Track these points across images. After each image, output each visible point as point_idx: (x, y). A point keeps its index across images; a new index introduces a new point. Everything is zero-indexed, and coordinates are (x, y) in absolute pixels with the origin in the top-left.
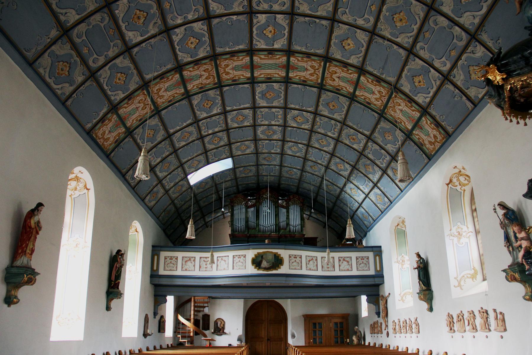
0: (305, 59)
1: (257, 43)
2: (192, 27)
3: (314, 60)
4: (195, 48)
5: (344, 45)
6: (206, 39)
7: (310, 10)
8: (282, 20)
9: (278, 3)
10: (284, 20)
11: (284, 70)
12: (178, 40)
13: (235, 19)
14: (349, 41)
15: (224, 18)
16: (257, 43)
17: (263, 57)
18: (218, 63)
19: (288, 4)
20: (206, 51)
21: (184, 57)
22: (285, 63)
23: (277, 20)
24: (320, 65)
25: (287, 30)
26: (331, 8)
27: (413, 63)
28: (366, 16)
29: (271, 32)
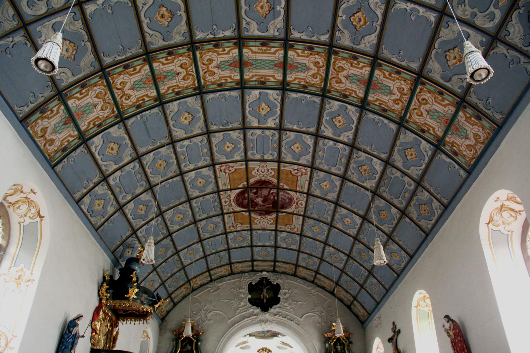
0: (224, 81)
1: (276, 97)
3: (213, 83)
6: (325, 118)
11: (245, 59)
16: (276, 97)
17: (272, 79)
18: (323, 84)
20: (331, 105)
21: (353, 112)
22: (245, 70)
23: (257, 121)
24: (204, 79)
25: (247, 111)
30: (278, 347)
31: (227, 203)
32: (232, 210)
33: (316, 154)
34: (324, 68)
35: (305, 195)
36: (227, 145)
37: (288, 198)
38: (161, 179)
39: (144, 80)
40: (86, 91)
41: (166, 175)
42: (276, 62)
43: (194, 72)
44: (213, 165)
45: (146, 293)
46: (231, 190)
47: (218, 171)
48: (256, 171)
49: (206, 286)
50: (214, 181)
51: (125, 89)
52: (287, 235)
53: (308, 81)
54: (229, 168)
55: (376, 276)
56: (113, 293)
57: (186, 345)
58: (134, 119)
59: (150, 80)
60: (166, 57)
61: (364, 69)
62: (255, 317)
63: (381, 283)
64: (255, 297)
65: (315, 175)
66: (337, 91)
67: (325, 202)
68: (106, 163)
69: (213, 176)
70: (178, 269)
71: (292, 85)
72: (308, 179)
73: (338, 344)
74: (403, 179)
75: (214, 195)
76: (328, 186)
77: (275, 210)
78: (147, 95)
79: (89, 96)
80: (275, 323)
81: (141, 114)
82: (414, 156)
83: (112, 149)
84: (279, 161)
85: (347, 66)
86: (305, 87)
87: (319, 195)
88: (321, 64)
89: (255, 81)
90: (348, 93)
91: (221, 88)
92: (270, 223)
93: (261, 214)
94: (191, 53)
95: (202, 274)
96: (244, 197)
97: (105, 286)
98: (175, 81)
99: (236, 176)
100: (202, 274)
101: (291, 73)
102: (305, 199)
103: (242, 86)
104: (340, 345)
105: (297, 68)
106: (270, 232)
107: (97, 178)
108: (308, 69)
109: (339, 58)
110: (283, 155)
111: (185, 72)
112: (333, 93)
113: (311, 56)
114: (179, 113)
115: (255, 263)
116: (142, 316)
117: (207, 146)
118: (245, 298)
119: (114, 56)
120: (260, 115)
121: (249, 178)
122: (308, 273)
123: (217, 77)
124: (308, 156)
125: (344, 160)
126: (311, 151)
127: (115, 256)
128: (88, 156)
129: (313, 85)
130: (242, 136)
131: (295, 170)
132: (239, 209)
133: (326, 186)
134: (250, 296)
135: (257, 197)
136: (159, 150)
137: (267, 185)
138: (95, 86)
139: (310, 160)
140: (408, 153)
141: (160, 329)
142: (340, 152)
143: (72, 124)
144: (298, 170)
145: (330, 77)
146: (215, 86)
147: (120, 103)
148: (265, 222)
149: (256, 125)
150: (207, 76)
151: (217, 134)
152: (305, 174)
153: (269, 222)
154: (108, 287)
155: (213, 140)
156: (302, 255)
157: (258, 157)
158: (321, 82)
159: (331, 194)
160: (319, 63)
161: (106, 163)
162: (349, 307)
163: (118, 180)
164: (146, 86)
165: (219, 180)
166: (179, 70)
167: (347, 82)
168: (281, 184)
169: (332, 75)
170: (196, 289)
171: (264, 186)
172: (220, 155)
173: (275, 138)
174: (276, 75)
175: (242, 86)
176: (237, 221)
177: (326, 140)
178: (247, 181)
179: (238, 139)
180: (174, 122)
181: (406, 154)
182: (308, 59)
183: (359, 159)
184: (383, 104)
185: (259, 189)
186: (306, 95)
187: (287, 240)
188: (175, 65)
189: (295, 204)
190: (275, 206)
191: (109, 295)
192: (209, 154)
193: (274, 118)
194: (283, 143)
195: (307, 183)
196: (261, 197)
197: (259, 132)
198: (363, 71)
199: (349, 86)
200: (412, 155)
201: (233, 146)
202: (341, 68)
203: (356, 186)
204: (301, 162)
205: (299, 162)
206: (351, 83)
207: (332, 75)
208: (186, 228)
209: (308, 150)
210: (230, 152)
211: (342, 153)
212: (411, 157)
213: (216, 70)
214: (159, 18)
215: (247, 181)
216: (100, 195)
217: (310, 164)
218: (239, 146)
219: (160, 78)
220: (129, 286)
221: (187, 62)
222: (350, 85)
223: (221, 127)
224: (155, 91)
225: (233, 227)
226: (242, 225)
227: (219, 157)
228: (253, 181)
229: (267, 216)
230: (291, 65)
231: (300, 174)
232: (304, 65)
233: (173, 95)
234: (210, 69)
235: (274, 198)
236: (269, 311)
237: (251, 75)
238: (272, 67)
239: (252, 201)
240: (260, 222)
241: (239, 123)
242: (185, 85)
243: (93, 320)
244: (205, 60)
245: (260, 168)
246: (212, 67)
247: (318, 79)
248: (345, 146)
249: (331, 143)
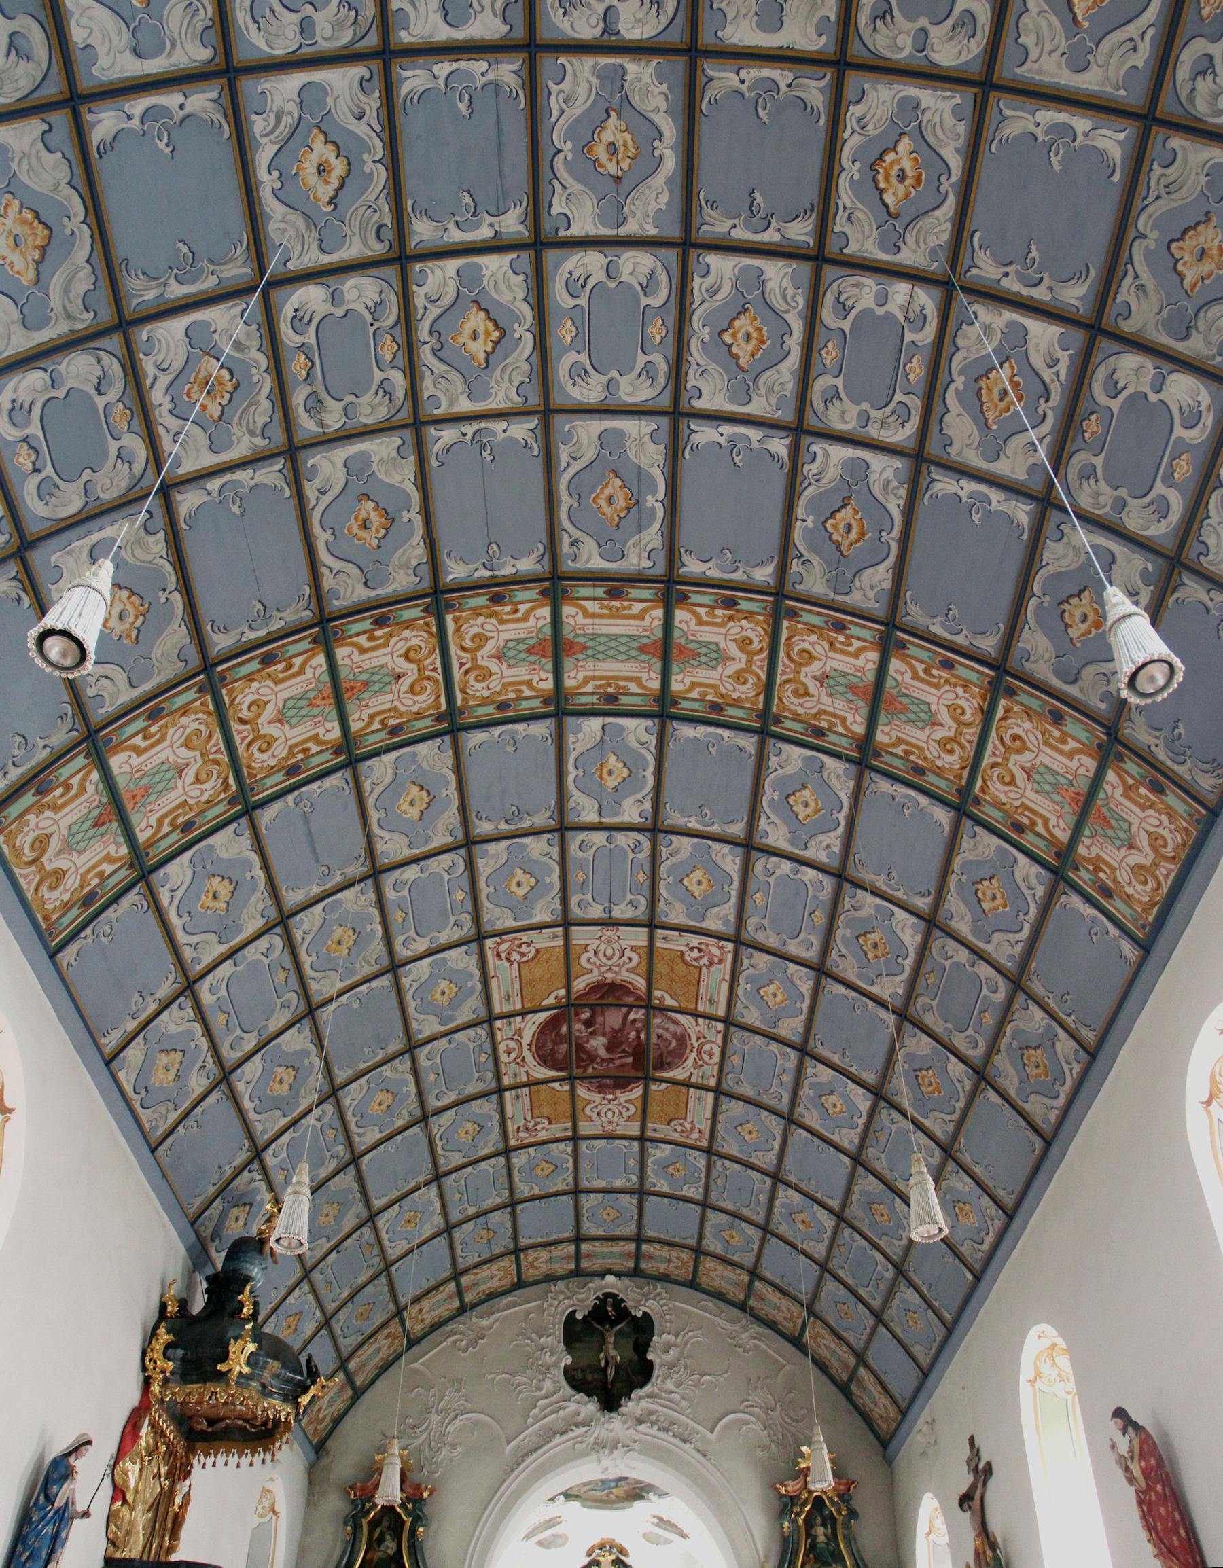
0: (512, 695)
2: (792, 842)
3: (485, 702)
4: (804, 787)
5: (424, 793)
9: (595, 848)
10: (579, 808)
12: (832, 834)
14: (414, 813)
17: (633, 688)
19: (572, 847)
20: (784, 756)
21: (839, 777)
24: (463, 691)
26: (480, 865)
27: (260, 907)
28: (405, 892)
29: (610, 773)
30: (647, 1537)
31: (513, 1056)
32: (524, 1078)
33: (749, 903)
35: (720, 1026)
36: (519, 879)
37: (674, 1035)
38: (340, 985)
40: (161, 727)
41: (352, 972)
44: (479, 937)
45: (276, 1358)
46: (523, 1013)
47: (490, 955)
48: (591, 954)
49: (448, 1328)
50: (479, 987)
52: (672, 1154)
54: (520, 946)
55: (917, 1280)
56: (183, 1360)
57: (381, 1540)
58: (277, 806)
59: (325, 694)
61: (862, 657)
62: (582, 1430)
63: (930, 1306)
64: (584, 1363)
65: (746, 962)
66: (797, 718)
67: (774, 1046)
68: (194, 939)
69: (477, 973)
70: (371, 1272)
71: (684, 704)
72: (727, 977)
73: (819, 1520)
74: (975, 969)
75: (479, 1030)
76: (778, 996)
77: (640, 1074)
79: (167, 743)
80: (640, 1452)
81: (296, 793)
82: (999, 901)
83: (215, 897)
84: (652, 924)
86: (716, 708)
87: (758, 1024)
89: (592, 693)
90: (824, 724)
91: (506, 714)
92: (625, 1114)
93: (601, 1089)
94: (432, 620)
95: (435, 1288)
96: (558, 1035)
97: (164, 1336)
98: (389, 697)
99: (538, 971)
100: (435, 1288)
102: (720, 1036)
103: (559, 707)
104: (824, 1525)
106: (626, 1143)
107: (168, 983)
108: (723, 658)
110: (662, 904)
111: (416, 671)
112: (788, 724)
115: (585, 1247)
116: (258, 1436)
117: (465, 882)
118: (555, 1365)
119: (240, 630)
120: (602, 787)
121: (573, 976)
122: (731, 1275)
123: (495, 684)
124: (727, 906)
125: (820, 918)
126: (734, 893)
127: (197, 1233)
128: (151, 918)
130: (555, 852)
131: (692, 949)
132: (543, 1073)
133: (775, 995)
134: (568, 1360)
135: (593, 1034)
136: (339, 896)
137: (619, 998)
138: (184, 714)
139: (732, 918)
140: (984, 894)
141: (310, 1483)
142: (810, 894)
143: (115, 824)
144: (700, 950)
146: (490, 709)
147: (244, 762)
148: (611, 1111)
149: (591, 817)
150: (472, 682)
151: (491, 847)
152: (720, 962)
153: (624, 1111)
154: (171, 1338)
155: (480, 863)
156: (714, 1218)
157: (596, 912)
159: (788, 1021)
161: (194, 939)
162: (844, 1389)
163: (223, 992)
165: (494, 983)
166: (402, 665)
168: (657, 993)
170: (418, 1341)
171: (611, 1001)
172: (498, 909)
173: (641, 856)
174: (644, 676)
175: (559, 707)
176: (537, 1112)
177: (774, 859)
178: (568, 986)
179: (546, 859)
180: (382, 814)
181: (980, 895)
183: (857, 914)
184: (913, 753)
185: (598, 1009)
186: (719, 731)
187: (671, 1169)
189: (694, 1055)
190: (641, 1063)
191: (170, 1365)
192: (469, 906)
193: (639, 796)
194: (663, 870)
195: (725, 986)
196: (604, 1035)
197: (599, 838)
198: (861, 662)
200: (994, 898)
201: (533, 881)
203: (854, 994)
204: (710, 924)
205: (704, 925)
208: (399, 1137)
209: (726, 888)
210: (525, 898)
211: (814, 897)
212: (992, 905)
214: (355, 530)
215: (568, 986)
216: (171, 1037)
217: (731, 931)
218: (547, 880)
219: (352, 688)
220: (231, 1334)
222: (828, 701)
223: (503, 826)
225: (527, 1129)
226: (550, 1123)
227: (497, 917)
228: (583, 985)
229: (618, 1093)
231: (705, 961)
233: (382, 735)
235: (638, 1037)
236: (623, 1409)
237: (581, 676)
239: (580, 1047)
240: (598, 1114)
241: (548, 814)
242: (415, 709)
243: (119, 1456)
245: (603, 947)
248: (820, 875)
249: (786, 866)
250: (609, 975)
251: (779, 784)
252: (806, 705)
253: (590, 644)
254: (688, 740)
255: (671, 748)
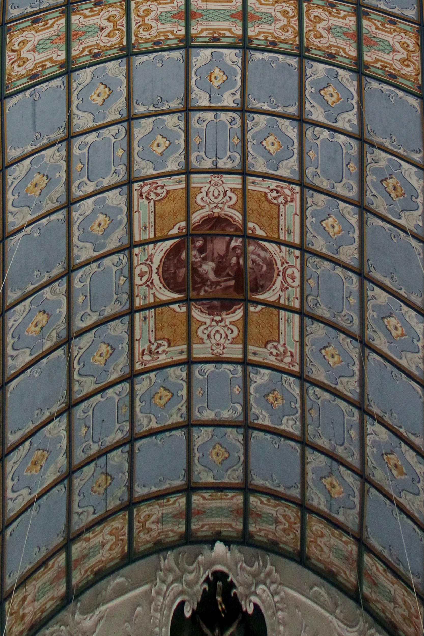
0: (162, 38)
1: (235, 59)
3: (147, 41)
7: (164, 120)
8: (200, 98)
13: (266, 104)
15: (279, 110)
16: (235, 59)
17: (228, 34)
18: (297, 39)
22: (193, 22)
23: (208, 97)
25: (193, 81)
34: (296, 18)
39: (54, 37)
42: (233, 12)
43: (125, 26)
51: (22, 51)
53: (277, 35)
59: (62, 37)
60: (92, 8)
66: (318, 48)
71: (256, 42)
78: (51, 60)
85: (324, 15)
86: (274, 44)
88: (291, 14)
89: (206, 37)
90: (334, 52)
91: (158, 47)
98: (96, 39)
101: (253, 26)
103: (188, 44)
105: (260, 18)
109: (312, 5)
111: (112, 26)
112: (313, 51)
113: (277, 4)
114: (90, 86)
123: (154, 32)
129: (284, 41)
145: (305, 31)
146: (150, 45)
150: (141, 31)
158: (295, 37)
160: (288, 13)
164: (55, 45)
166: (105, 23)
167: (330, 36)
169: (307, 27)
174: (234, 28)
175: (188, 44)
182: (274, 7)
186: (276, 55)
188: (101, 18)
199: (333, 41)
202: (317, 18)
206: (334, 37)
207: (307, 27)
213: (153, 24)
219: (77, 34)
221: (118, 14)
224: (64, 53)
230: (253, 16)
232: (269, 15)
234: (147, 22)
237: (199, 28)
238: (228, 18)
242: (109, 45)
244: (142, 11)
246: (149, 20)
247: (290, 32)
250: (216, 210)
251: (313, 84)
252: (322, 42)
253: (204, 13)
254: (259, 60)
255: (250, 64)
